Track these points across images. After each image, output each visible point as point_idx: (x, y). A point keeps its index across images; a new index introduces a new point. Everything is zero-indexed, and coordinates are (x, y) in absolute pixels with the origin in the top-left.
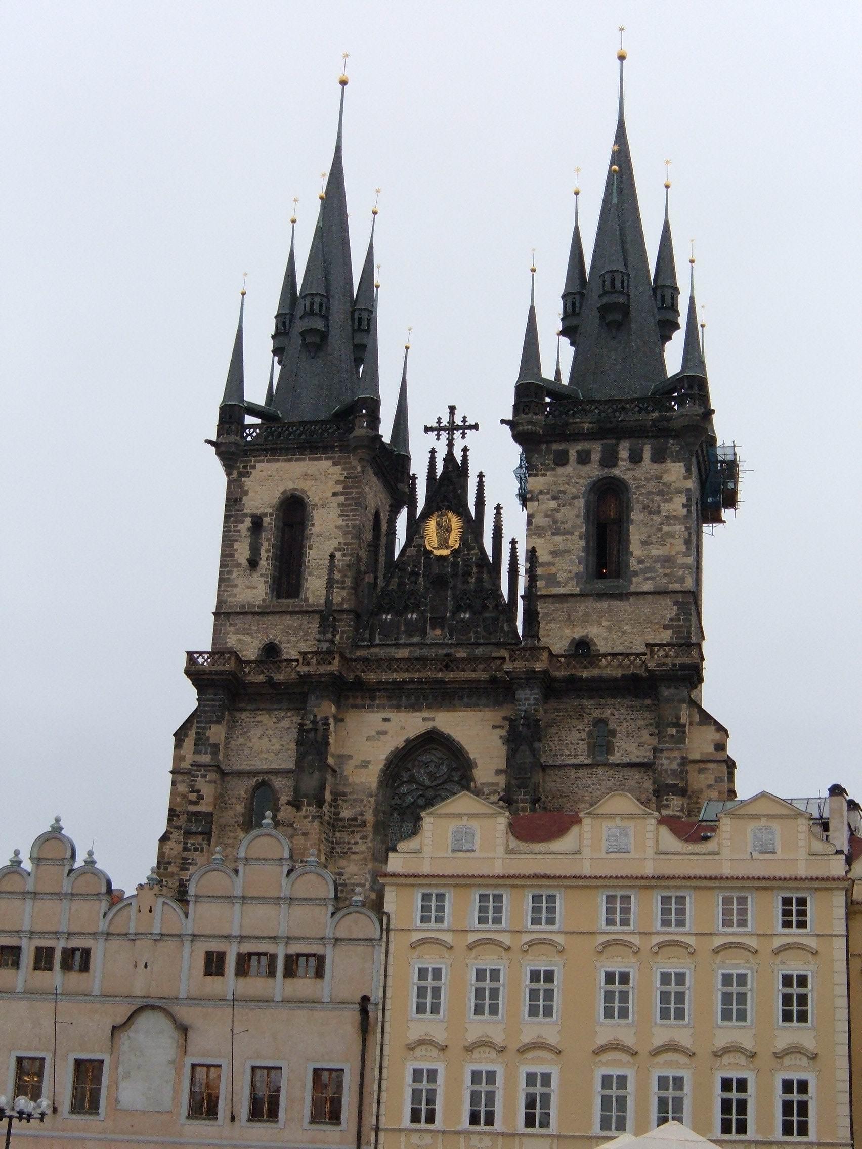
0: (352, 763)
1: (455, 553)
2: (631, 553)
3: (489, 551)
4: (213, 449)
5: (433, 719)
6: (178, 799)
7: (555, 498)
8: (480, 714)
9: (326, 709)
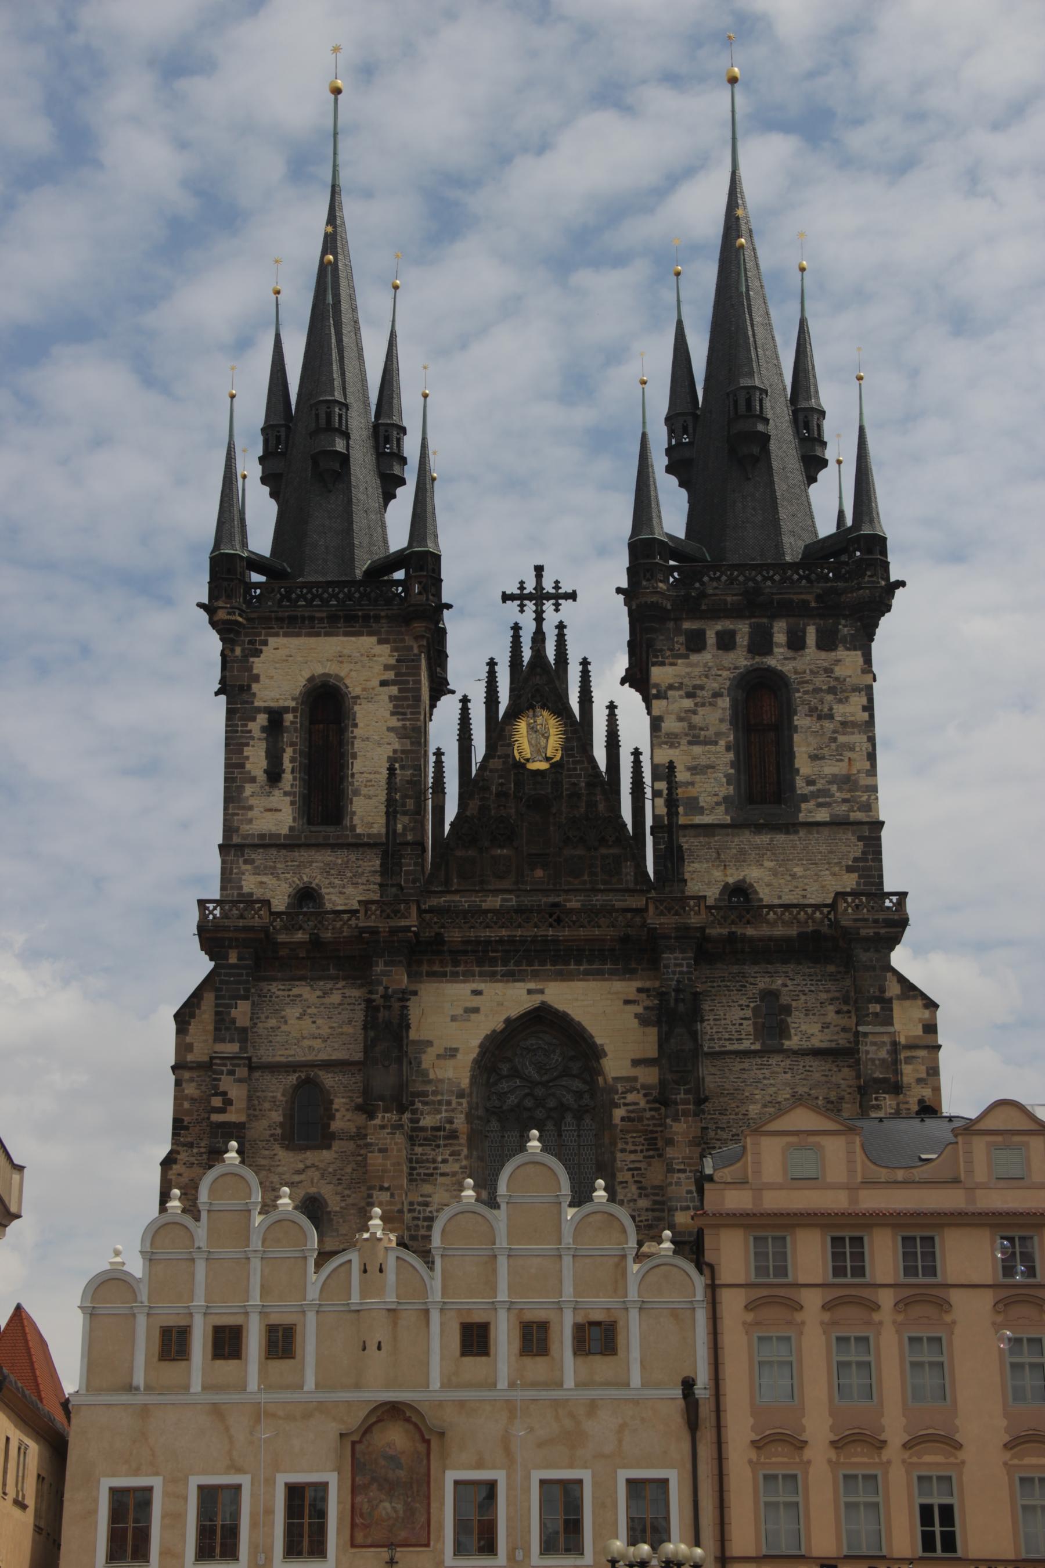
2: (798, 770)
3: (603, 767)
4: (204, 616)
6: (186, 1105)
7: (690, 695)
8: (606, 983)
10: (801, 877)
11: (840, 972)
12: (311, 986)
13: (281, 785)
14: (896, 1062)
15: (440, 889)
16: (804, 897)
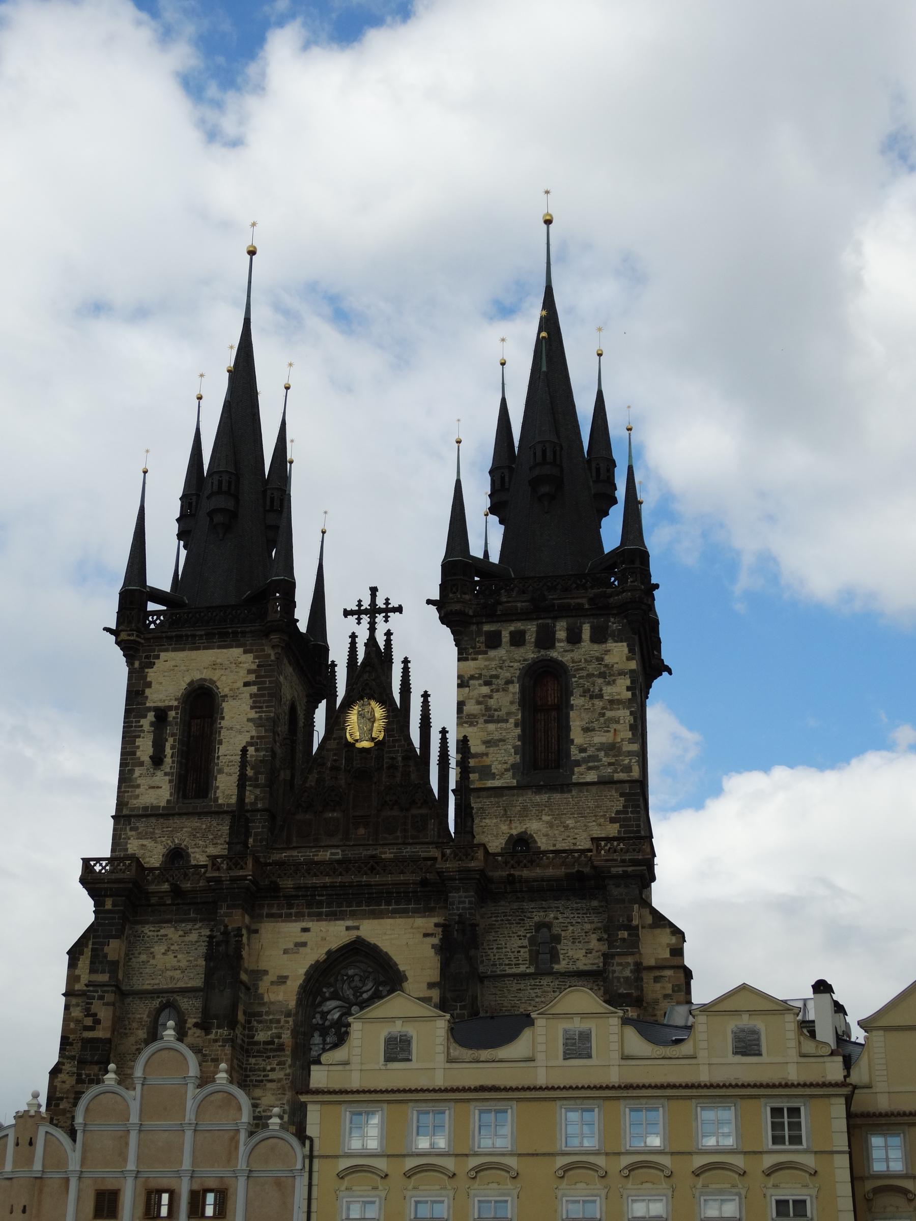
0: (267, 979)
1: (379, 744)
2: (573, 741)
5: (357, 928)
6: (72, 1025)
7: (487, 683)
8: (410, 920)
9: (237, 919)
10: (572, 828)
11: (602, 906)
12: (175, 927)
13: (162, 767)
14: (639, 979)
15: (282, 846)
16: (575, 844)
